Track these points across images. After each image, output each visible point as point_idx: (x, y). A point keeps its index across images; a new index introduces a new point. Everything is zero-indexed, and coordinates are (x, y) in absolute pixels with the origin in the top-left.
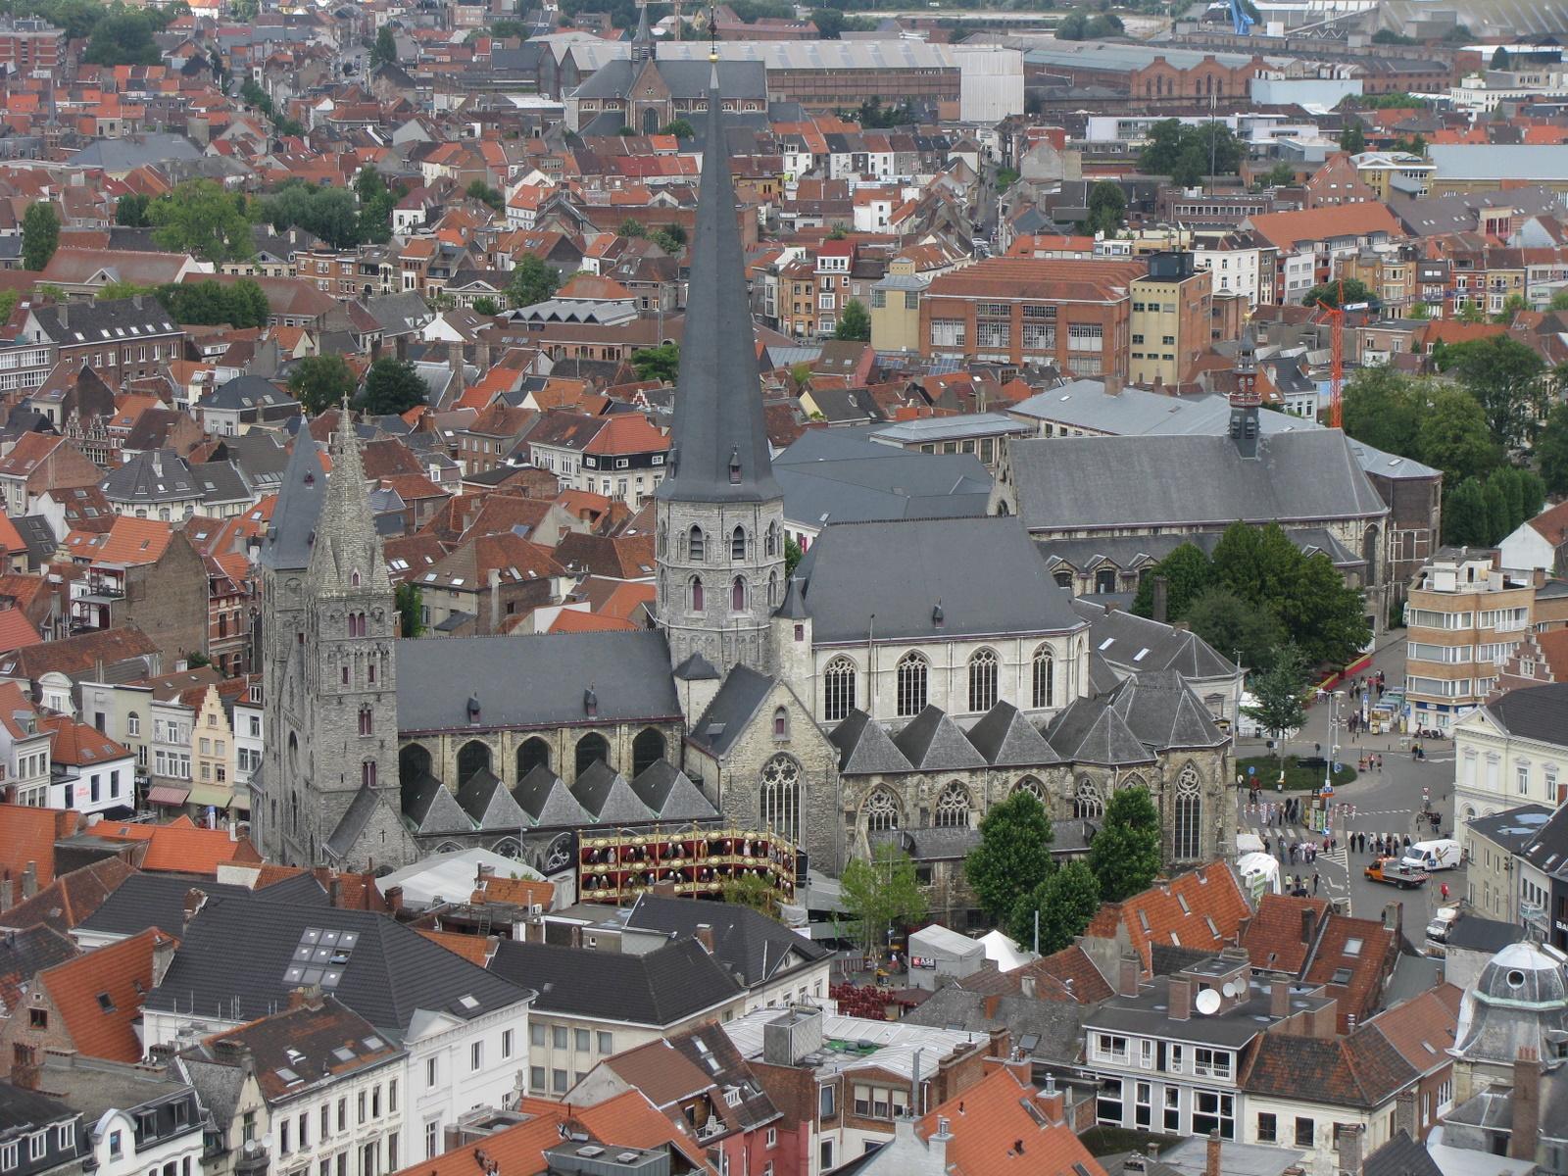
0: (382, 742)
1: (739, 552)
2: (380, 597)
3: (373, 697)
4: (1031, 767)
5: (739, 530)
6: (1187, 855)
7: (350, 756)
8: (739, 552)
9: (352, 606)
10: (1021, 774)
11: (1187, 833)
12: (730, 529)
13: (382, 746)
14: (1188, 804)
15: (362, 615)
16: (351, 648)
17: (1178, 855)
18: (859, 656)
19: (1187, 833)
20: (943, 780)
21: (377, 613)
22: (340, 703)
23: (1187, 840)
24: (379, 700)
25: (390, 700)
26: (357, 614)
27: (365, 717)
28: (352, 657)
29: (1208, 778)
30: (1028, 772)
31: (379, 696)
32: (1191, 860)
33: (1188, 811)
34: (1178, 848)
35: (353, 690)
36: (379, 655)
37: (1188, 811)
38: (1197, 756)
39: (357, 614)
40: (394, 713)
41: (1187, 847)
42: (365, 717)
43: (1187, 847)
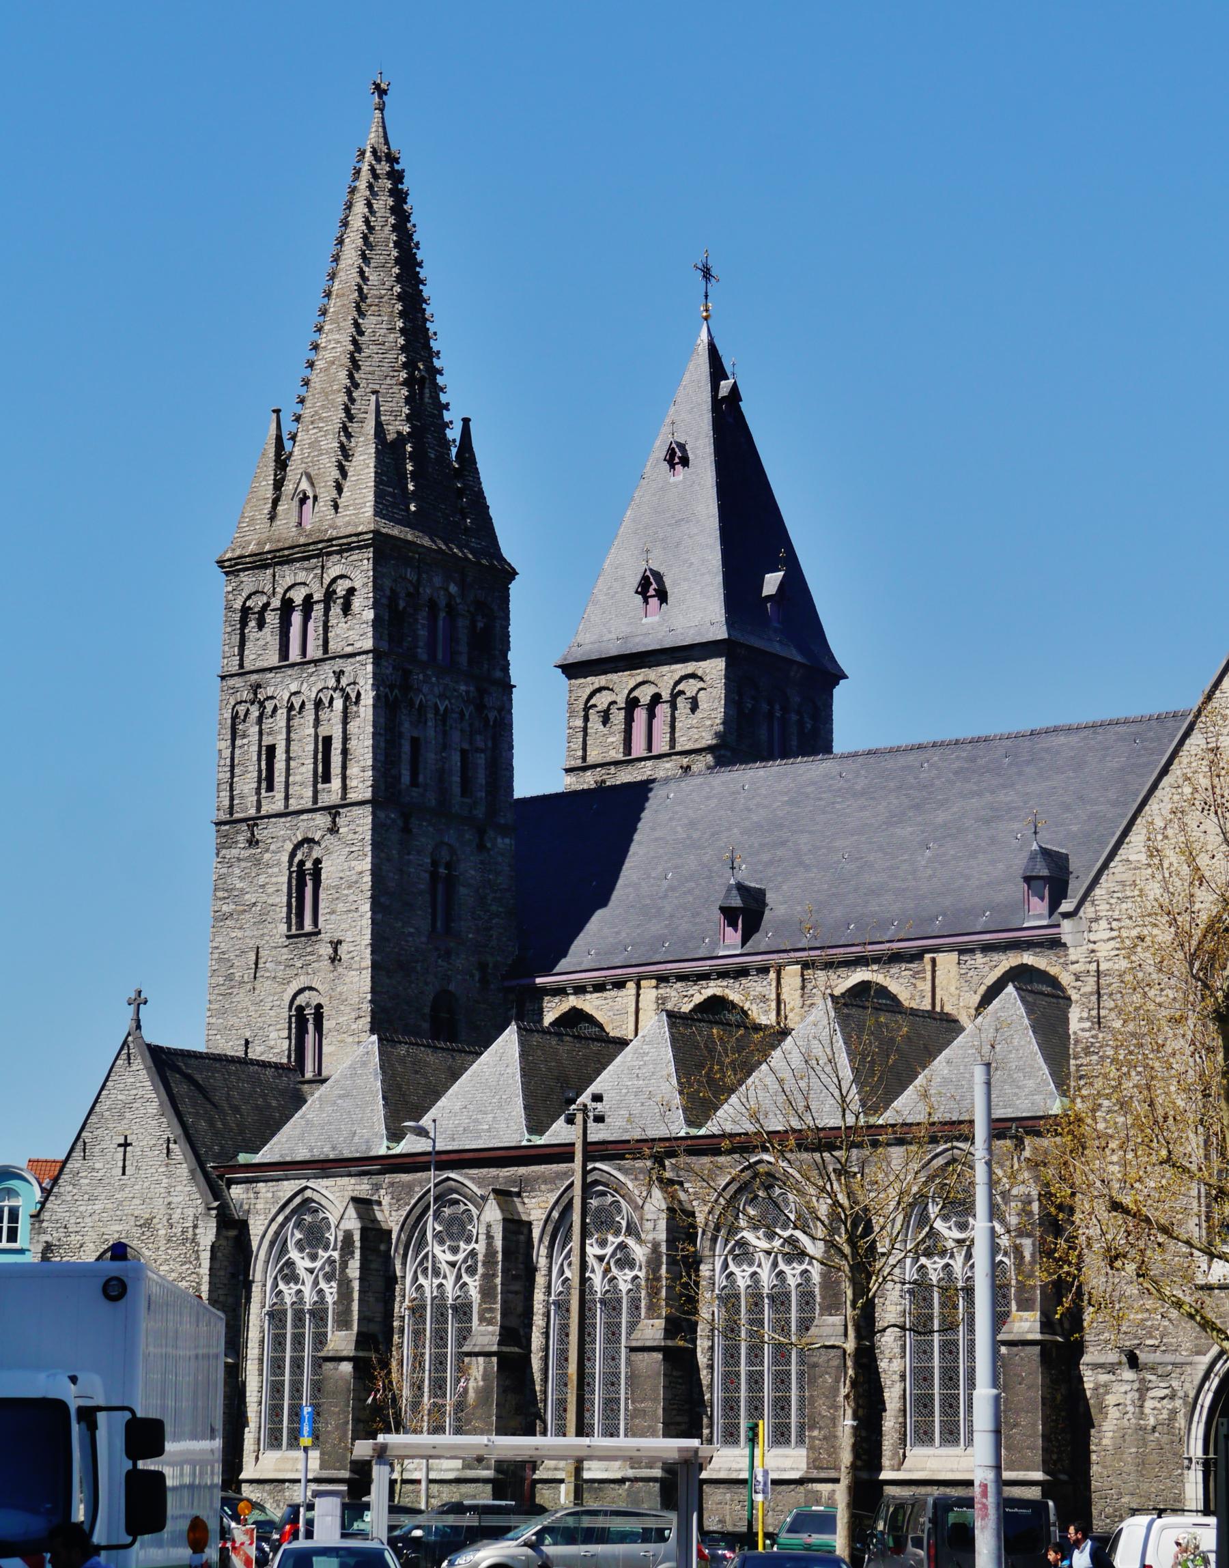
0: (336, 944)
2: (345, 546)
3: (322, 820)
7: (265, 986)
9: (287, 575)
13: (335, 959)
15: (308, 602)
16: (281, 688)
21: (341, 588)
22: (253, 842)
24: (333, 830)
25: (359, 824)
26: (298, 596)
27: (305, 879)
28: (282, 713)
31: (333, 811)
35: (279, 806)
36: (338, 704)
39: (298, 596)
40: (366, 864)
42: (305, 879)
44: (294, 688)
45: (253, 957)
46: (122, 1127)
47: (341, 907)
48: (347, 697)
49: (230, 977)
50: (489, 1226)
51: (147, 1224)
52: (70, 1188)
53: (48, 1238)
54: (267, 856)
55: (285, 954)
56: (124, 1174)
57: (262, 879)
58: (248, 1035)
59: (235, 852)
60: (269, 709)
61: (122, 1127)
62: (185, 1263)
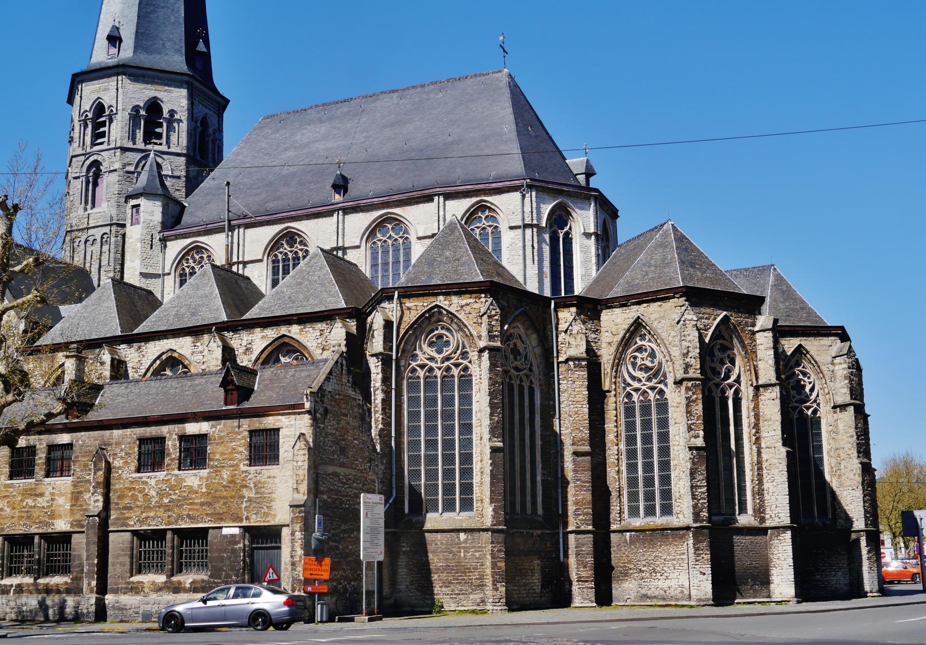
1: (98, 136)
4: (287, 320)
5: (99, 109)
6: (650, 511)
8: (98, 136)
10: (272, 333)
11: (648, 467)
12: (87, 106)
14: (646, 409)
17: (634, 512)
18: (216, 244)
19: (648, 467)
20: (154, 349)
23: (649, 482)
29: (676, 353)
30: (283, 330)
32: (659, 520)
33: (646, 425)
34: (633, 497)
37: (646, 425)
38: (651, 312)
41: (650, 497)
43: (650, 497)
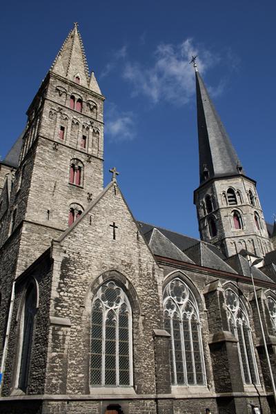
44: (75, 117)
45: (53, 184)
46: (112, 218)
47: (91, 184)
48: (94, 130)
49: (42, 186)
50: (264, 300)
51: (129, 265)
52: (82, 235)
53: (67, 256)
54: (61, 156)
55: (67, 189)
56: (114, 238)
57: (58, 162)
58: (49, 209)
59: (44, 148)
60: (65, 117)
61: (112, 218)
62: (149, 289)
